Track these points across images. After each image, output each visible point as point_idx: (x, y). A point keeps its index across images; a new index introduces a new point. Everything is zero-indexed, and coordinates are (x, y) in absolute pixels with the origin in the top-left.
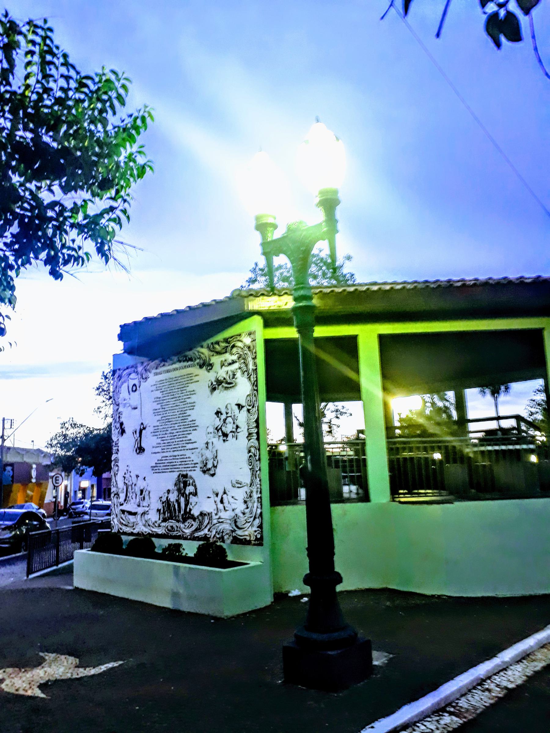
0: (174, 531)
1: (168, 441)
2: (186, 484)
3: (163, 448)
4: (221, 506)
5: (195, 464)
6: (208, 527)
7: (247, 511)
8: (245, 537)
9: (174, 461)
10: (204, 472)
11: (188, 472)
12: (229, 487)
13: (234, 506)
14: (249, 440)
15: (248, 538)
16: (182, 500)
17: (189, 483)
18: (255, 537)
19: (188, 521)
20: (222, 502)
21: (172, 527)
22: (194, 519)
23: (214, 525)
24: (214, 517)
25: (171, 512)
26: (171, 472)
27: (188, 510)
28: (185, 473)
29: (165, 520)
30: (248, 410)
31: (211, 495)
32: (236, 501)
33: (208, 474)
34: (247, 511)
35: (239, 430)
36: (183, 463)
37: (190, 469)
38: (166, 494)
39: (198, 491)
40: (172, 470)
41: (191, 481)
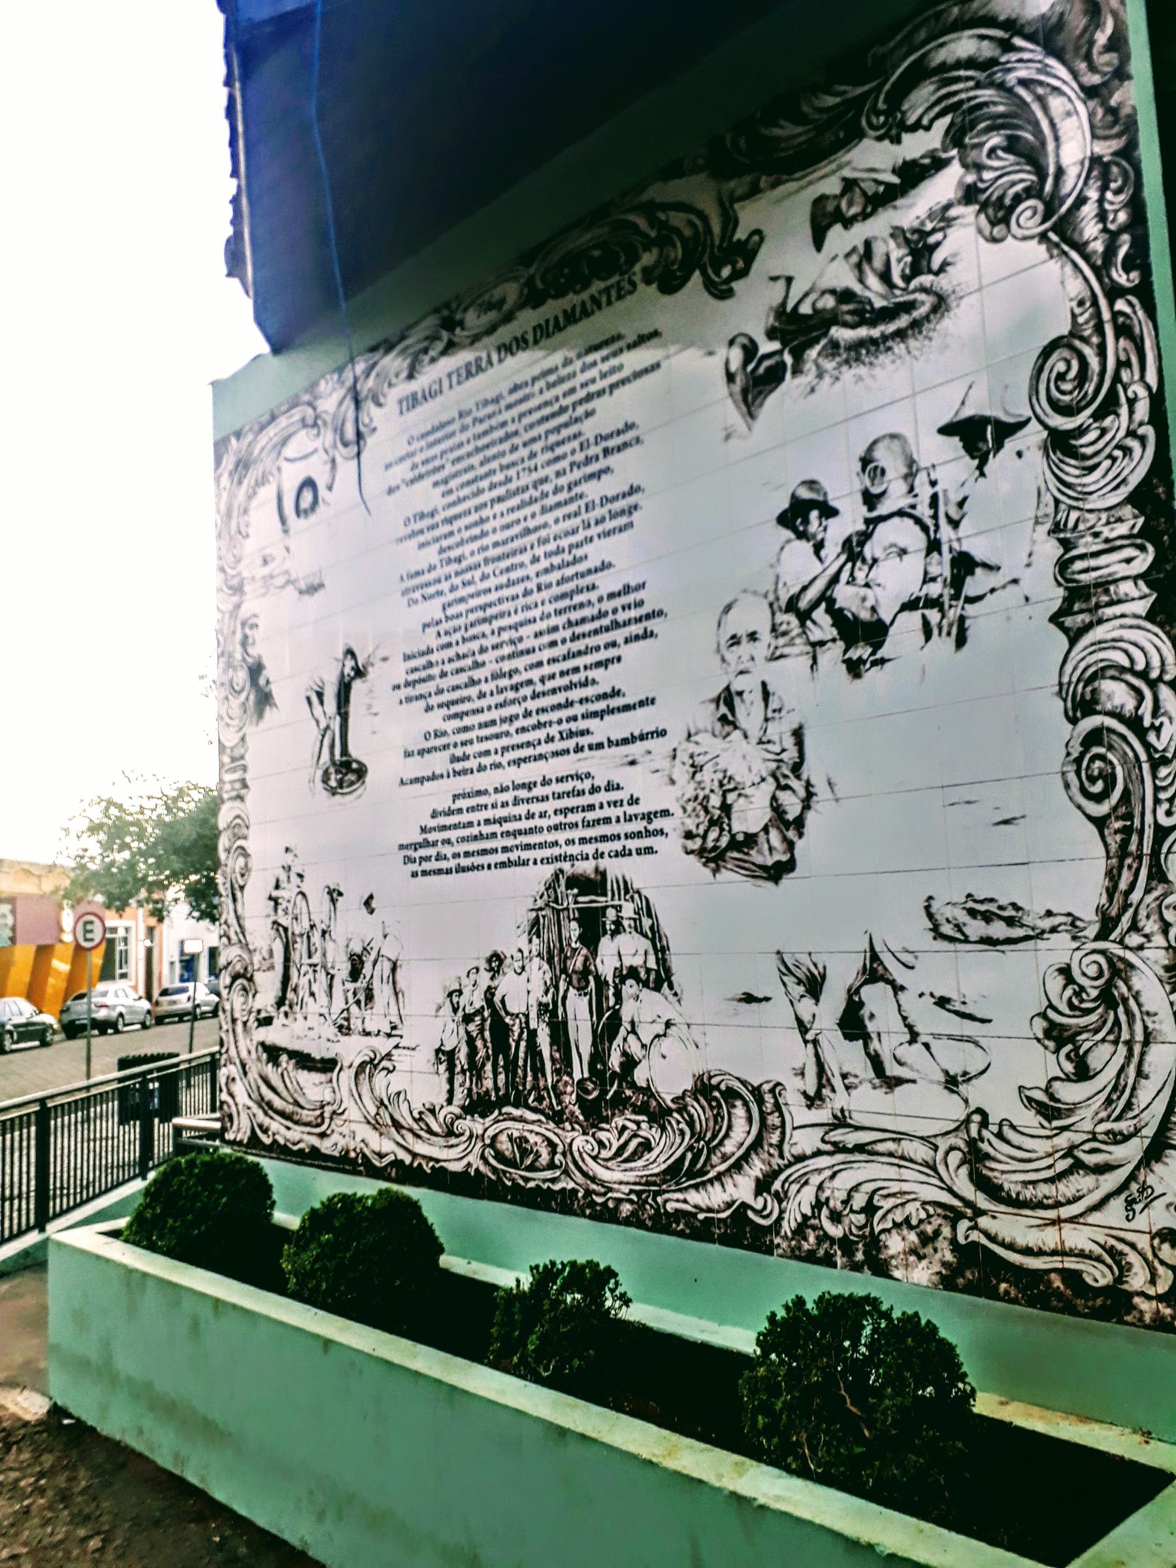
0: (532, 1168)
1: (486, 717)
2: (593, 928)
3: (459, 752)
4: (845, 1056)
5: (649, 817)
6: (757, 1167)
7: (1068, 1093)
9: (522, 810)
10: (713, 858)
11: (604, 863)
13: (955, 1058)
14: (1074, 636)
16: (578, 1008)
17: (618, 923)
19: (619, 1121)
20: (853, 1023)
21: (520, 1142)
22: (659, 1116)
25: (511, 1066)
26: (503, 865)
27: (615, 1061)
28: (586, 868)
29: (479, 1106)
31: (767, 982)
32: (970, 1029)
33: (741, 865)
34: (1068, 1093)
35: (974, 584)
36: (572, 818)
37: (617, 846)
38: (484, 979)
39: (675, 963)
40: (513, 856)
41: (628, 910)
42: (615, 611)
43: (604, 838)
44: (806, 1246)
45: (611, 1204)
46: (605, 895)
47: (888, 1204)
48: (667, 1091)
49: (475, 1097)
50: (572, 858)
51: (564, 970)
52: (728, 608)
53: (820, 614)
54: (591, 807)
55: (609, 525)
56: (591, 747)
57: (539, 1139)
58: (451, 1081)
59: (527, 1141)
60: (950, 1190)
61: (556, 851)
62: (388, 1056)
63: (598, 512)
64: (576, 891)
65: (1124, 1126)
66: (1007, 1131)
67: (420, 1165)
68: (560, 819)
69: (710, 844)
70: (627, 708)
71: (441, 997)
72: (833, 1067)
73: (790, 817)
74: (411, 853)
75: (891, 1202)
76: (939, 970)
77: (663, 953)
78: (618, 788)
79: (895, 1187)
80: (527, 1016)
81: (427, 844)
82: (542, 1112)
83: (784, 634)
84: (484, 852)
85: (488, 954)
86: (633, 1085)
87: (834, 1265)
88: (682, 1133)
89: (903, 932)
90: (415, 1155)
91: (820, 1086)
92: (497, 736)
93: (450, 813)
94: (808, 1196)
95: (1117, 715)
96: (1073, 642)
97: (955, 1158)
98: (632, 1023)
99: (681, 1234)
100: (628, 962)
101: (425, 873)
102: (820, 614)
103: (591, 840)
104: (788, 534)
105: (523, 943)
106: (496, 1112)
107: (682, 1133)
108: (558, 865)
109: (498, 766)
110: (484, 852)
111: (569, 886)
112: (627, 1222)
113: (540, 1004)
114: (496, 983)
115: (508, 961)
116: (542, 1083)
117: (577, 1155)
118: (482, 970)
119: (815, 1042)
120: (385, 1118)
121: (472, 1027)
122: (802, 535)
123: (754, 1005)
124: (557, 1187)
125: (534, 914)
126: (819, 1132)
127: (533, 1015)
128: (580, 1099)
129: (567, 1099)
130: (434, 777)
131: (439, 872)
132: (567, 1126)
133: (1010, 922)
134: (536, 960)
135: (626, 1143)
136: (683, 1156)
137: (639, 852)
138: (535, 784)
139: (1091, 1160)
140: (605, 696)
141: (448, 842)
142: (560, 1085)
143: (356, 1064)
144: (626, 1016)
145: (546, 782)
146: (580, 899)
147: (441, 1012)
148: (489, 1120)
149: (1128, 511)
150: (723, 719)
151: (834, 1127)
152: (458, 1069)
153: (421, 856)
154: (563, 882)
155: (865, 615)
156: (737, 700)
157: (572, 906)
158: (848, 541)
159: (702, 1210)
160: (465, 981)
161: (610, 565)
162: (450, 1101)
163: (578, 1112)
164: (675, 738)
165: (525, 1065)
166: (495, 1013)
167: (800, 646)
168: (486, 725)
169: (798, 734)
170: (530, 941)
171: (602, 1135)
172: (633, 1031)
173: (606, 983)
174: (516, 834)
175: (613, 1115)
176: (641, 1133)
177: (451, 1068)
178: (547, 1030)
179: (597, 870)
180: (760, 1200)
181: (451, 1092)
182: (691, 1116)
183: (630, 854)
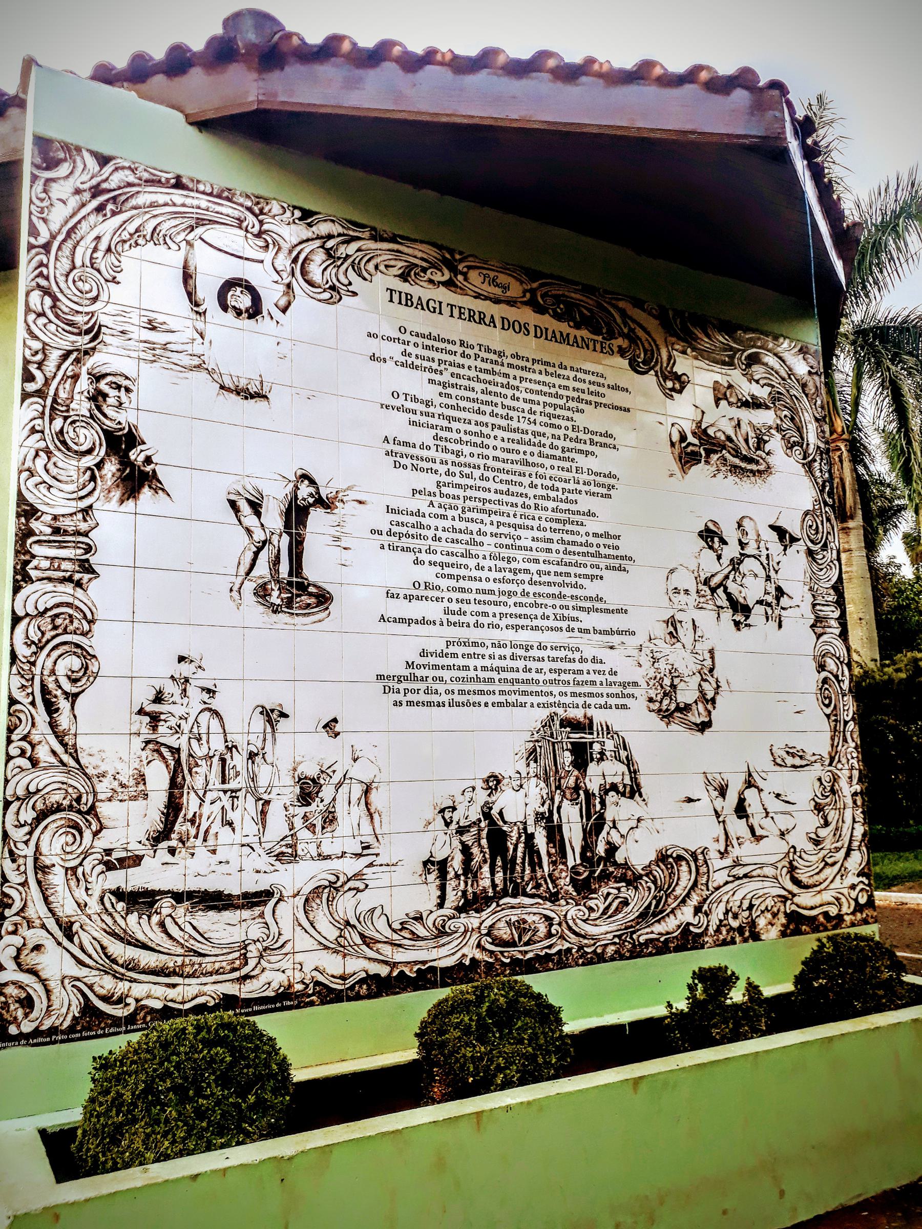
1: (484, 585)
2: (582, 757)
3: (454, 606)
4: (738, 827)
5: (624, 685)
6: (695, 899)
7: (823, 833)
8: (825, 908)
9: (520, 664)
10: (667, 716)
11: (590, 712)
13: (784, 823)
14: (819, 636)
15: (833, 911)
17: (602, 753)
18: (853, 903)
19: (604, 890)
20: (741, 810)
21: (521, 927)
22: (632, 880)
23: (717, 889)
24: (716, 862)
25: (509, 866)
26: (500, 705)
27: (601, 849)
28: (577, 714)
29: (473, 903)
30: (810, 553)
31: (698, 790)
33: (683, 723)
34: (823, 833)
35: (784, 601)
36: (564, 677)
37: (601, 701)
38: (482, 796)
39: (642, 780)
40: (512, 698)
41: (610, 745)
43: (591, 695)
44: (721, 937)
45: (599, 950)
49: (470, 897)
50: (565, 706)
52: (672, 571)
53: (720, 591)
54: (581, 672)
56: (580, 630)
57: (536, 918)
58: (442, 888)
59: (525, 922)
61: (551, 699)
62: (358, 876)
63: (585, 477)
64: (568, 729)
65: (839, 845)
66: (803, 855)
67: (402, 972)
68: (554, 676)
69: (664, 708)
70: (608, 611)
71: (430, 813)
72: (732, 835)
73: (709, 697)
75: (760, 900)
76: (777, 781)
77: (635, 772)
79: (761, 892)
81: (415, 678)
82: (539, 896)
83: (704, 596)
84: (481, 692)
85: (485, 776)
86: (615, 864)
89: (762, 763)
91: (727, 846)
92: (496, 604)
93: (442, 655)
94: (722, 908)
96: (818, 639)
97: (785, 870)
98: (614, 822)
99: (651, 955)
100: (609, 780)
101: (410, 703)
102: (720, 591)
105: (521, 766)
106: (494, 905)
108: (553, 709)
109: (497, 626)
110: (481, 692)
112: (612, 959)
114: (493, 798)
115: (505, 782)
116: (539, 875)
117: (571, 922)
118: (478, 789)
119: (724, 822)
120: (353, 935)
121: (465, 838)
122: (711, 548)
124: (553, 951)
125: (532, 744)
126: (726, 871)
128: (573, 881)
129: (561, 882)
130: (424, 622)
132: (563, 902)
133: (801, 757)
134: (534, 781)
135: (610, 904)
136: (650, 903)
137: (617, 707)
138: (532, 647)
139: (830, 861)
140: (591, 599)
141: (441, 679)
143: (306, 890)
144: (609, 816)
145: (540, 647)
147: (430, 827)
148: (484, 914)
149: (832, 592)
150: (671, 633)
152: (451, 874)
153: (406, 686)
155: (741, 600)
156: (678, 625)
158: (732, 560)
160: (459, 798)
161: (594, 515)
162: (441, 905)
165: (523, 863)
166: (492, 822)
168: (484, 592)
169: (711, 652)
170: (528, 765)
171: (591, 903)
172: (615, 827)
173: (594, 795)
178: (544, 833)
179: (585, 716)
181: (442, 898)
182: (655, 877)
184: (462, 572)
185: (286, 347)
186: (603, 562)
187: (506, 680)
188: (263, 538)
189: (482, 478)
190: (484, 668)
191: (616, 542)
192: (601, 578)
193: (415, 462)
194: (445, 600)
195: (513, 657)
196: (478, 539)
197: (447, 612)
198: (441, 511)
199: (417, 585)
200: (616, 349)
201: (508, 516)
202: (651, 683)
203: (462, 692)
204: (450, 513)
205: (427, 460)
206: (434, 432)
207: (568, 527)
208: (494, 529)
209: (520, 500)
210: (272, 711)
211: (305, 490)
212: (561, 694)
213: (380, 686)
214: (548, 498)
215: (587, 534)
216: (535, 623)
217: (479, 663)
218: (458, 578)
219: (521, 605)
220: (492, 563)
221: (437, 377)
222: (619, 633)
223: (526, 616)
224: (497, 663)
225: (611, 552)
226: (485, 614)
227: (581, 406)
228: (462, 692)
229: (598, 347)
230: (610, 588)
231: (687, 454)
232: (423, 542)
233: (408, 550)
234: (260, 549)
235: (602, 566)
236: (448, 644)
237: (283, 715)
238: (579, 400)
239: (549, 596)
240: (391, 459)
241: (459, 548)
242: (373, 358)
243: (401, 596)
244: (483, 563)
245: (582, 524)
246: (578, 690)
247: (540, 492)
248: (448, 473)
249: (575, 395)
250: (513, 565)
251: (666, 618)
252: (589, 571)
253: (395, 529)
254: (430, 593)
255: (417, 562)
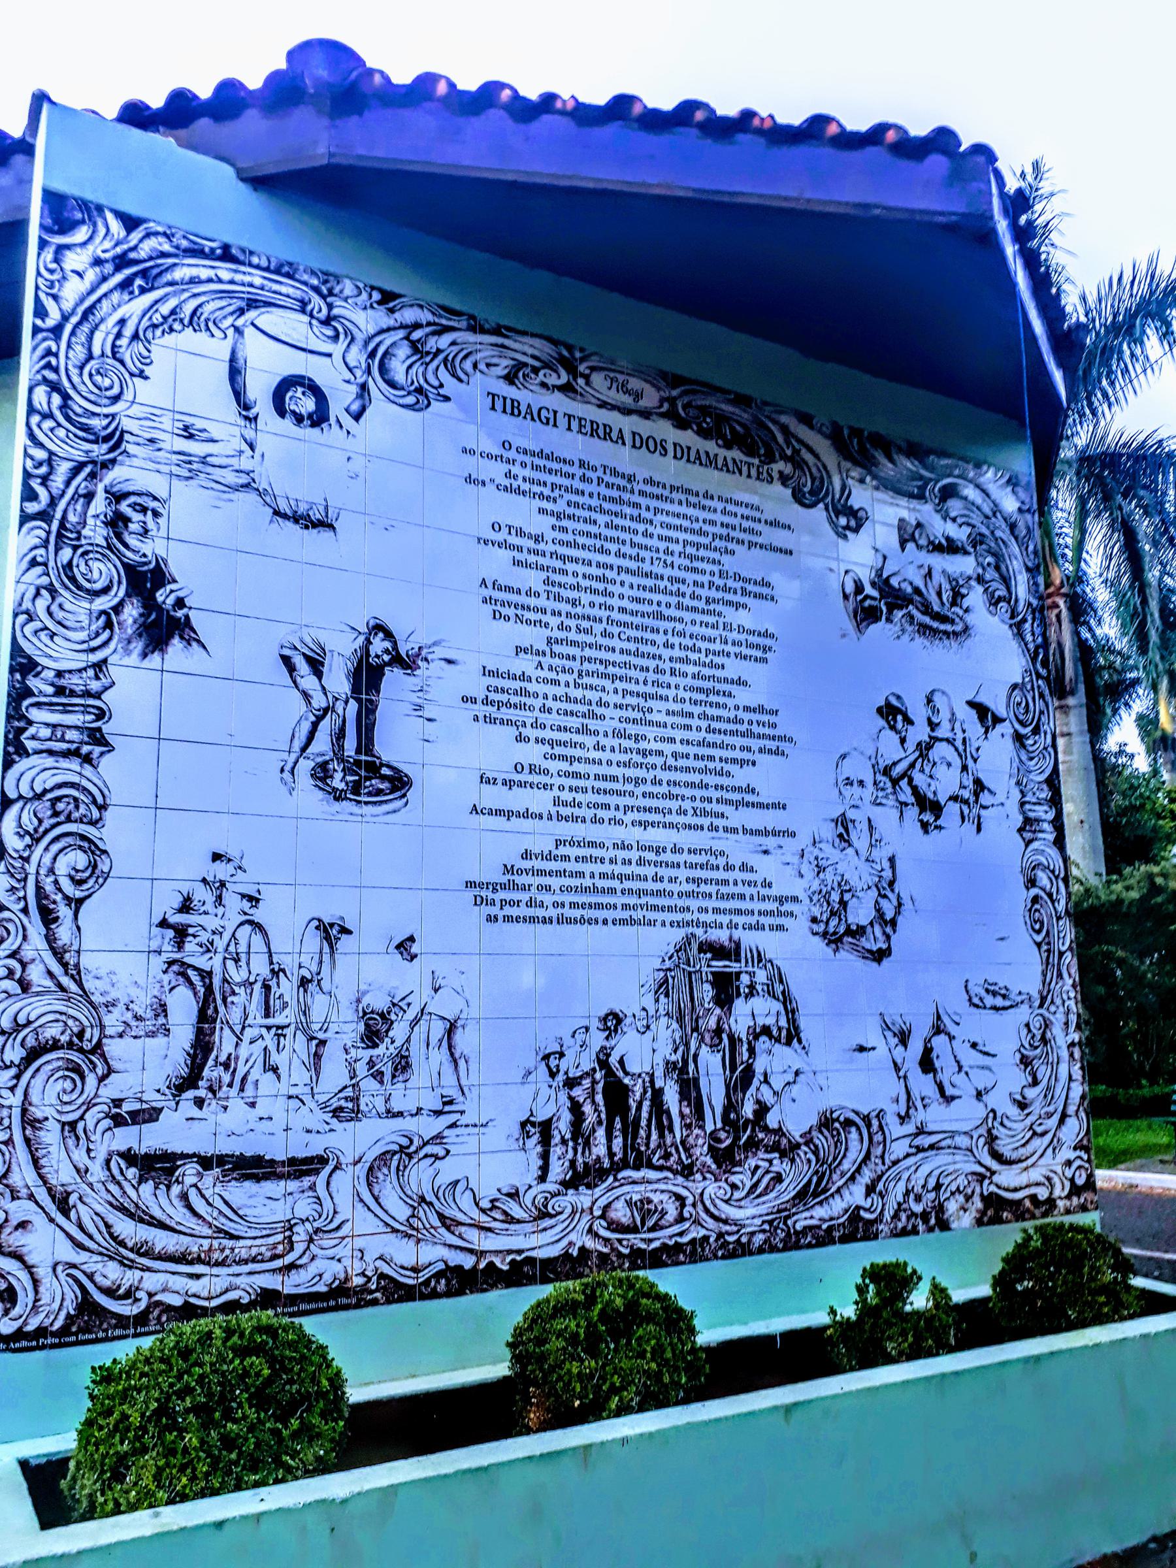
0: (656, 1228)
1: (603, 770)
2: (726, 990)
3: (566, 796)
4: (923, 1085)
5: (781, 900)
6: (866, 1176)
7: (1031, 1093)
8: (1033, 1190)
9: (649, 871)
10: (834, 940)
11: (736, 934)
12: (956, 1003)
13: (981, 1080)
14: (1028, 843)
15: (1043, 1193)
17: (752, 987)
18: (1067, 1184)
19: (752, 1162)
20: (927, 1064)
21: (643, 1208)
22: (788, 1151)
23: (895, 1163)
24: (895, 1129)
25: (631, 1129)
26: (623, 922)
28: (721, 936)
30: (1019, 738)
31: (873, 1037)
32: (988, 1061)
33: (855, 948)
34: (1031, 1093)
35: (985, 798)
36: (704, 888)
37: (752, 920)
38: (597, 1039)
39: (803, 1023)
40: (638, 914)
41: (761, 976)
42: (750, 723)
43: (739, 912)
44: (900, 1225)
45: (744, 1240)
46: (739, 961)
47: (946, 1181)
48: (795, 1131)
49: (580, 1168)
50: (706, 925)
51: (695, 1029)
52: (844, 757)
53: (904, 783)
54: (725, 882)
55: (746, 651)
56: (726, 830)
57: (665, 1197)
58: (545, 1156)
59: (650, 1201)
60: (980, 1163)
61: (688, 917)
62: (438, 1138)
63: (734, 635)
64: (709, 955)
65: (1051, 1109)
66: (1006, 1122)
67: (491, 1264)
69: (831, 930)
70: (761, 806)
71: (531, 1060)
72: (916, 1094)
73: (888, 917)
74: (486, 893)
75: (950, 1178)
76: (974, 1025)
77: (793, 1012)
78: (752, 870)
79: (951, 1168)
80: (652, 1076)
81: (515, 887)
82: (669, 1169)
83: (883, 789)
84: (599, 906)
85: (602, 1013)
86: (766, 1129)
87: (917, 1233)
88: (809, 1161)
90: (483, 1253)
91: (908, 1108)
92: (619, 793)
93: (550, 857)
94: (901, 1188)
95: (1044, 890)
96: (1027, 846)
97: (982, 1140)
98: (765, 1075)
99: (809, 1246)
100: (761, 1021)
101: (508, 919)
102: (904, 783)
103: (724, 912)
104: (882, 723)
105: (648, 1001)
106: (611, 1179)
107: (809, 1161)
108: (690, 930)
109: (620, 822)
110: (599, 906)
111: (701, 950)
112: (761, 1251)
113: (667, 1063)
114: (613, 1042)
115: (628, 1021)
116: (669, 1141)
117: (708, 1203)
118: (593, 1029)
119: (905, 1077)
121: (579, 1093)
122: (893, 728)
123: (865, 1054)
124: (685, 1239)
125: (662, 974)
126: (907, 1141)
127: (659, 1073)
128: (711, 1149)
129: (697, 1152)
130: (527, 815)
131: (533, 920)
132: (698, 1176)
133: (1004, 997)
134: (664, 1021)
135: (759, 1181)
136: (810, 1181)
137: (771, 928)
139: (1039, 1130)
140: (739, 789)
141: (548, 888)
142: (691, 1140)
143: (370, 1157)
144: (759, 1066)
145: (676, 850)
146: (714, 963)
147: (532, 1078)
148: (598, 1191)
150: (840, 836)
151: (917, 1135)
152: (557, 1139)
153: (499, 897)
154: (695, 947)
155: (931, 796)
156: (850, 825)
157: (705, 969)
158: (919, 744)
159: (824, 1221)
160: (568, 1041)
161: (745, 684)
162: (542, 1179)
163: (709, 1160)
164: (803, 840)
165: (649, 1126)
166: (610, 1073)
167: (891, 801)
168: (605, 778)
169: (892, 860)
170: (657, 1001)
171: (735, 1179)
172: (766, 1081)
173: (740, 1040)
174: (640, 893)
175: (746, 1158)
176: (773, 1169)
177: (546, 1140)
178: (677, 1088)
180: (869, 1200)
181: (545, 1169)
182: (816, 1146)
183: (763, 929)
184: (578, 752)
185: (358, 464)
186: (755, 744)
187: (631, 891)
188: (324, 705)
189: (605, 634)
190: (603, 876)
191: (773, 719)
192: (754, 764)
193: (519, 612)
194: (555, 788)
195: (641, 862)
196: (599, 711)
197: (557, 802)
198: (553, 675)
199: (519, 768)
200: (775, 475)
201: (637, 682)
202: (815, 898)
203: (573, 905)
204: (563, 678)
205: (536, 610)
206: (544, 575)
207: (713, 698)
208: (618, 699)
209: (652, 664)
210: (332, 925)
211: (379, 645)
212: (701, 910)
213: (469, 895)
214: (687, 661)
215: (737, 708)
216: (668, 819)
217: (598, 868)
218: (571, 760)
219: (651, 795)
220: (615, 742)
221: (549, 506)
222: (775, 833)
223: (657, 810)
224: (619, 869)
225: (767, 731)
226: (607, 807)
227: (730, 546)
228: (573, 905)
229: (754, 472)
230: (766, 777)
231: (863, 609)
232: (528, 713)
233: (510, 722)
234: (319, 719)
235: (755, 748)
236: (558, 843)
237: (345, 931)
238: (728, 538)
239: (688, 785)
240: (489, 608)
241: (574, 722)
242: (469, 479)
243: (499, 781)
244: (604, 741)
245: (730, 695)
246: (722, 905)
247: (677, 653)
248: (561, 627)
249: (724, 531)
250: (643, 745)
251: (835, 815)
252: (738, 754)
253: (493, 696)
254: (536, 779)
255: (520, 738)
